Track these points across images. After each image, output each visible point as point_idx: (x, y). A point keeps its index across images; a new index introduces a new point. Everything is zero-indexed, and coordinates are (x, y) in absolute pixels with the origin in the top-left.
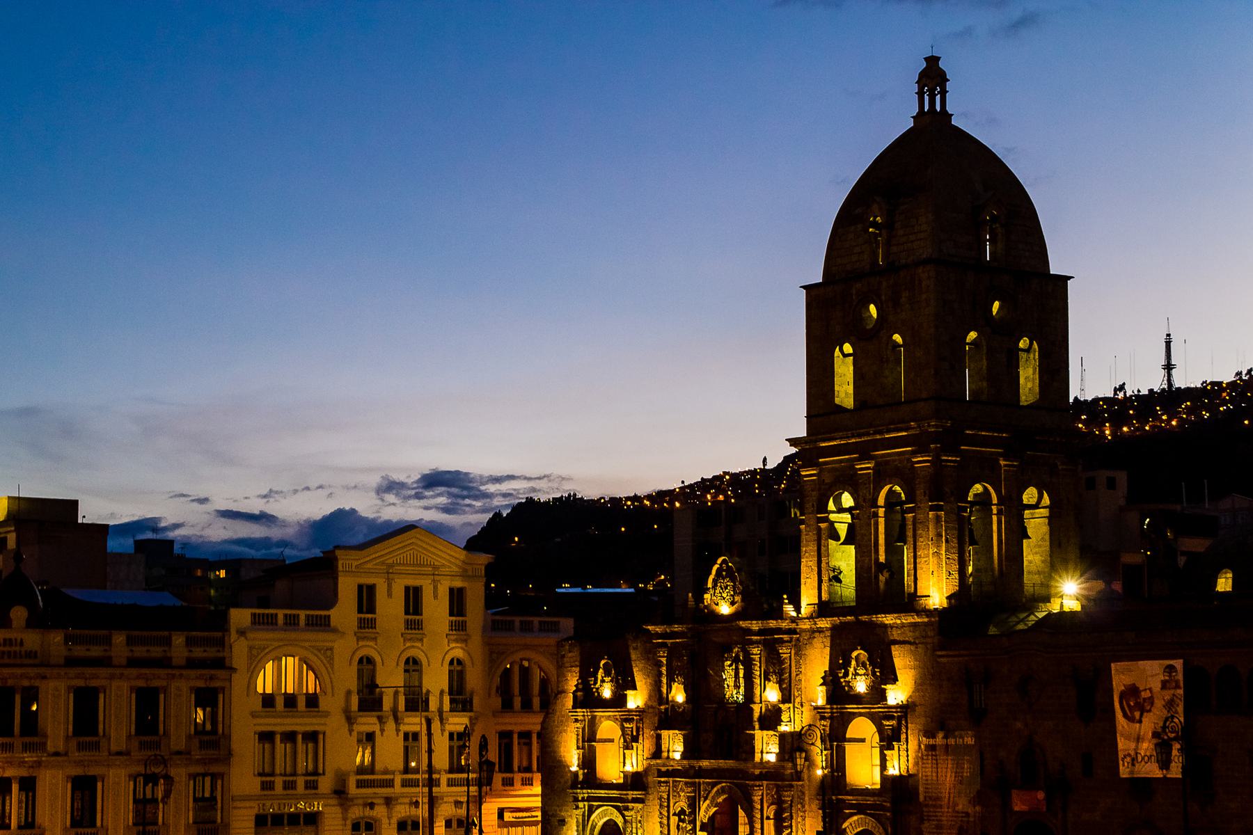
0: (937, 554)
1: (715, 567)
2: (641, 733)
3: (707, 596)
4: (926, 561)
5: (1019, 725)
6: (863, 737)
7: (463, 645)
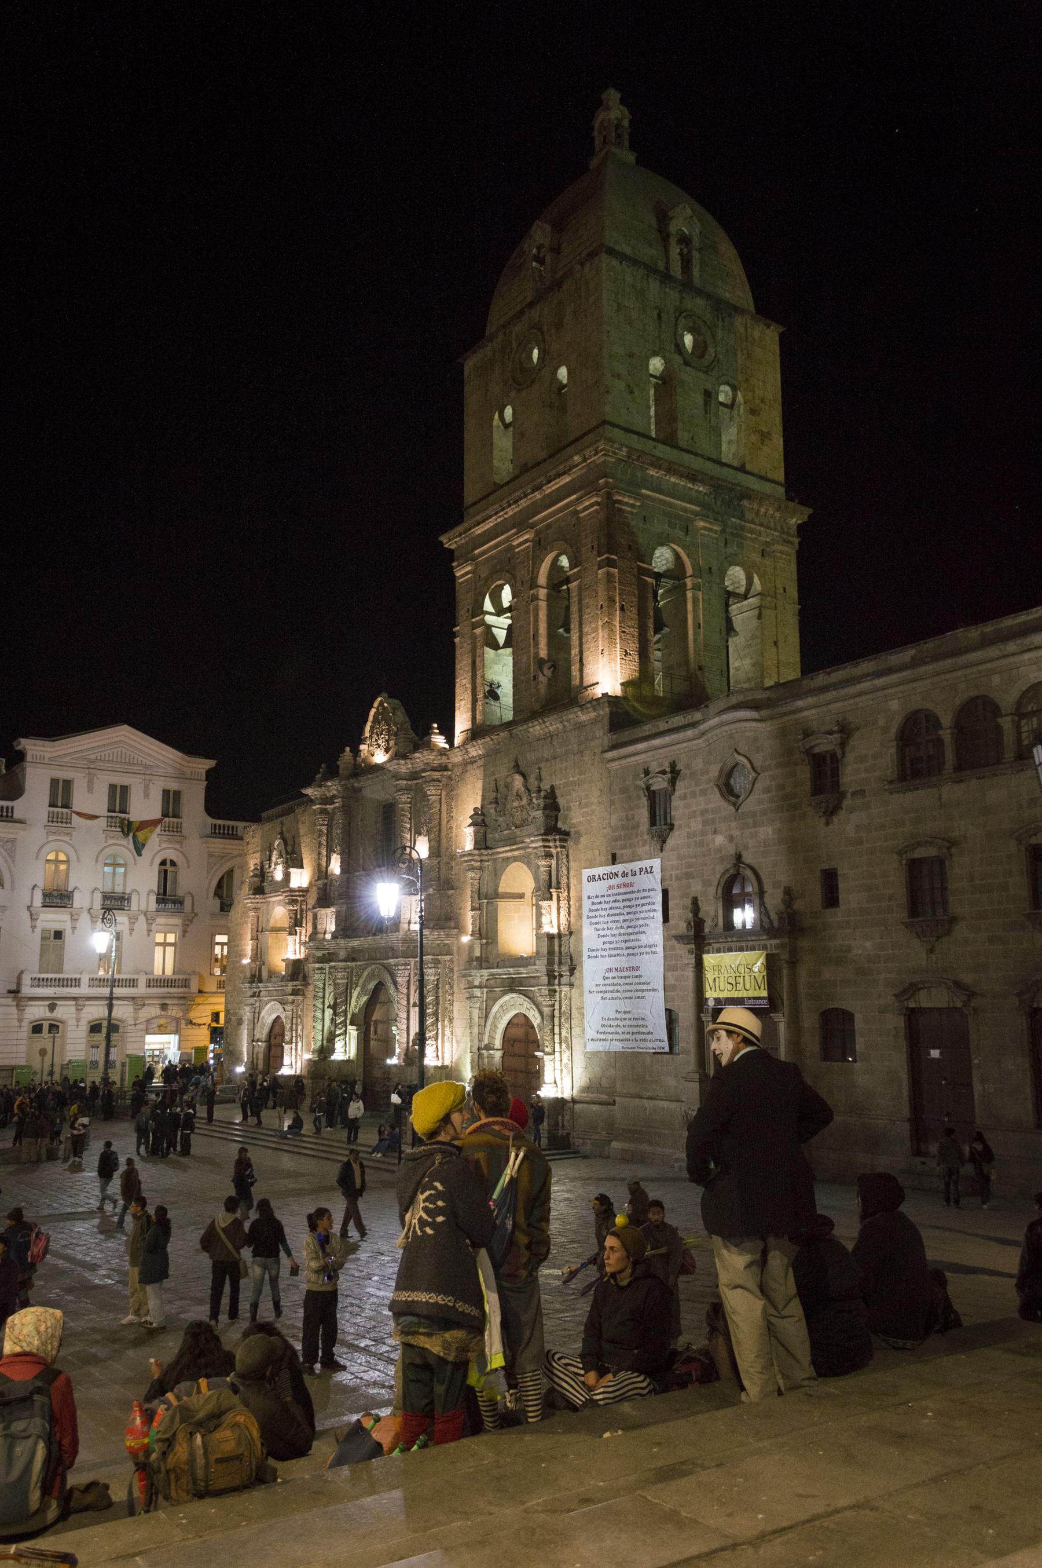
0: (609, 625)
1: (373, 711)
2: (304, 915)
3: (362, 747)
4: (594, 638)
5: (719, 840)
6: (521, 892)
7: (177, 846)
